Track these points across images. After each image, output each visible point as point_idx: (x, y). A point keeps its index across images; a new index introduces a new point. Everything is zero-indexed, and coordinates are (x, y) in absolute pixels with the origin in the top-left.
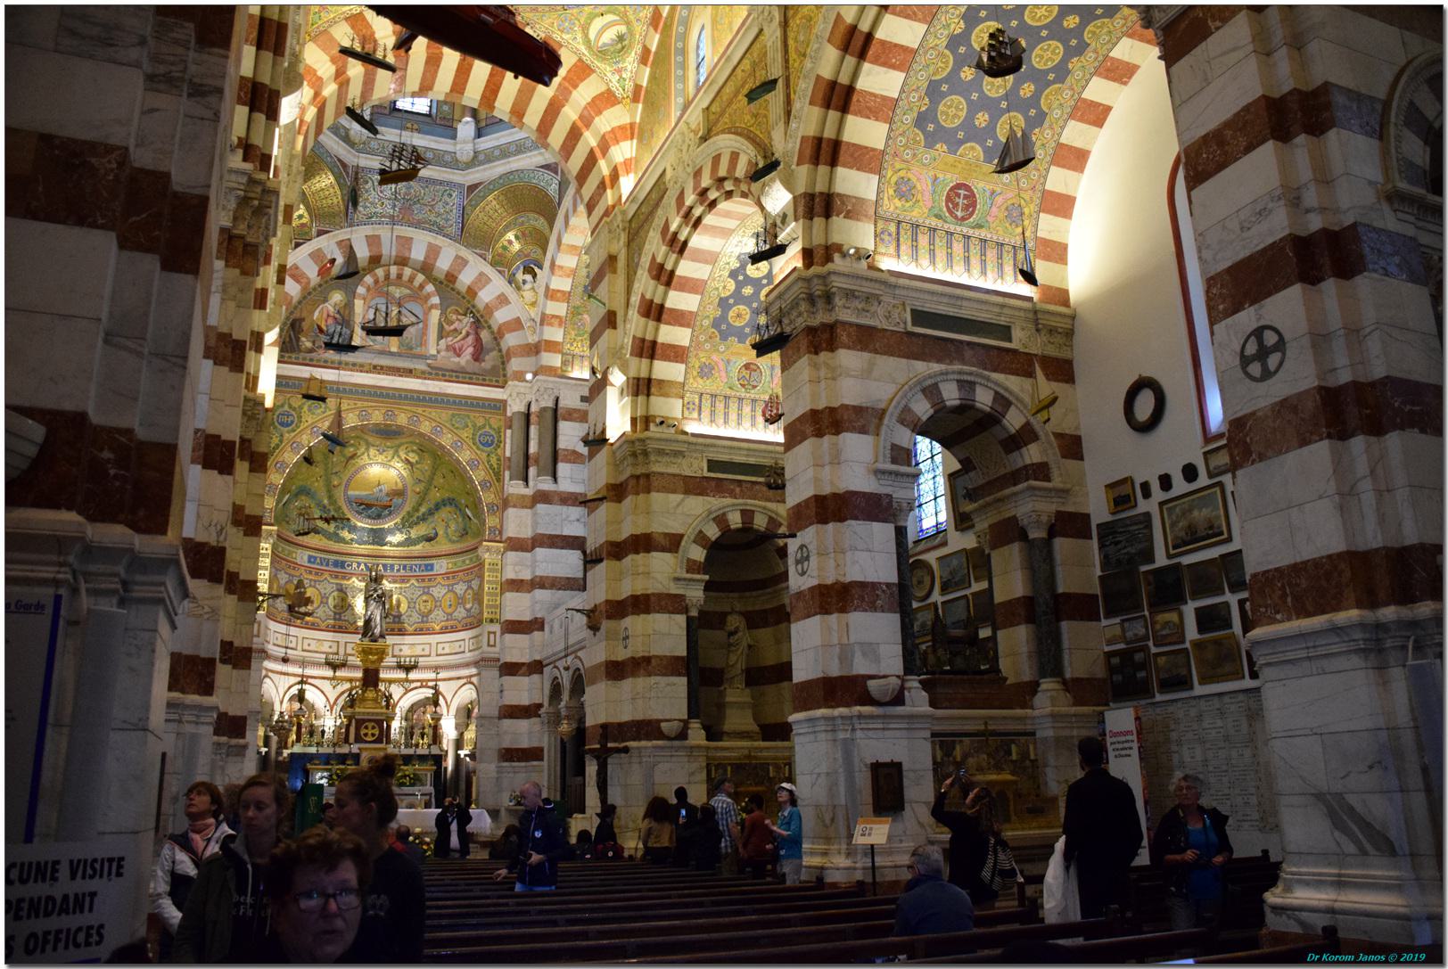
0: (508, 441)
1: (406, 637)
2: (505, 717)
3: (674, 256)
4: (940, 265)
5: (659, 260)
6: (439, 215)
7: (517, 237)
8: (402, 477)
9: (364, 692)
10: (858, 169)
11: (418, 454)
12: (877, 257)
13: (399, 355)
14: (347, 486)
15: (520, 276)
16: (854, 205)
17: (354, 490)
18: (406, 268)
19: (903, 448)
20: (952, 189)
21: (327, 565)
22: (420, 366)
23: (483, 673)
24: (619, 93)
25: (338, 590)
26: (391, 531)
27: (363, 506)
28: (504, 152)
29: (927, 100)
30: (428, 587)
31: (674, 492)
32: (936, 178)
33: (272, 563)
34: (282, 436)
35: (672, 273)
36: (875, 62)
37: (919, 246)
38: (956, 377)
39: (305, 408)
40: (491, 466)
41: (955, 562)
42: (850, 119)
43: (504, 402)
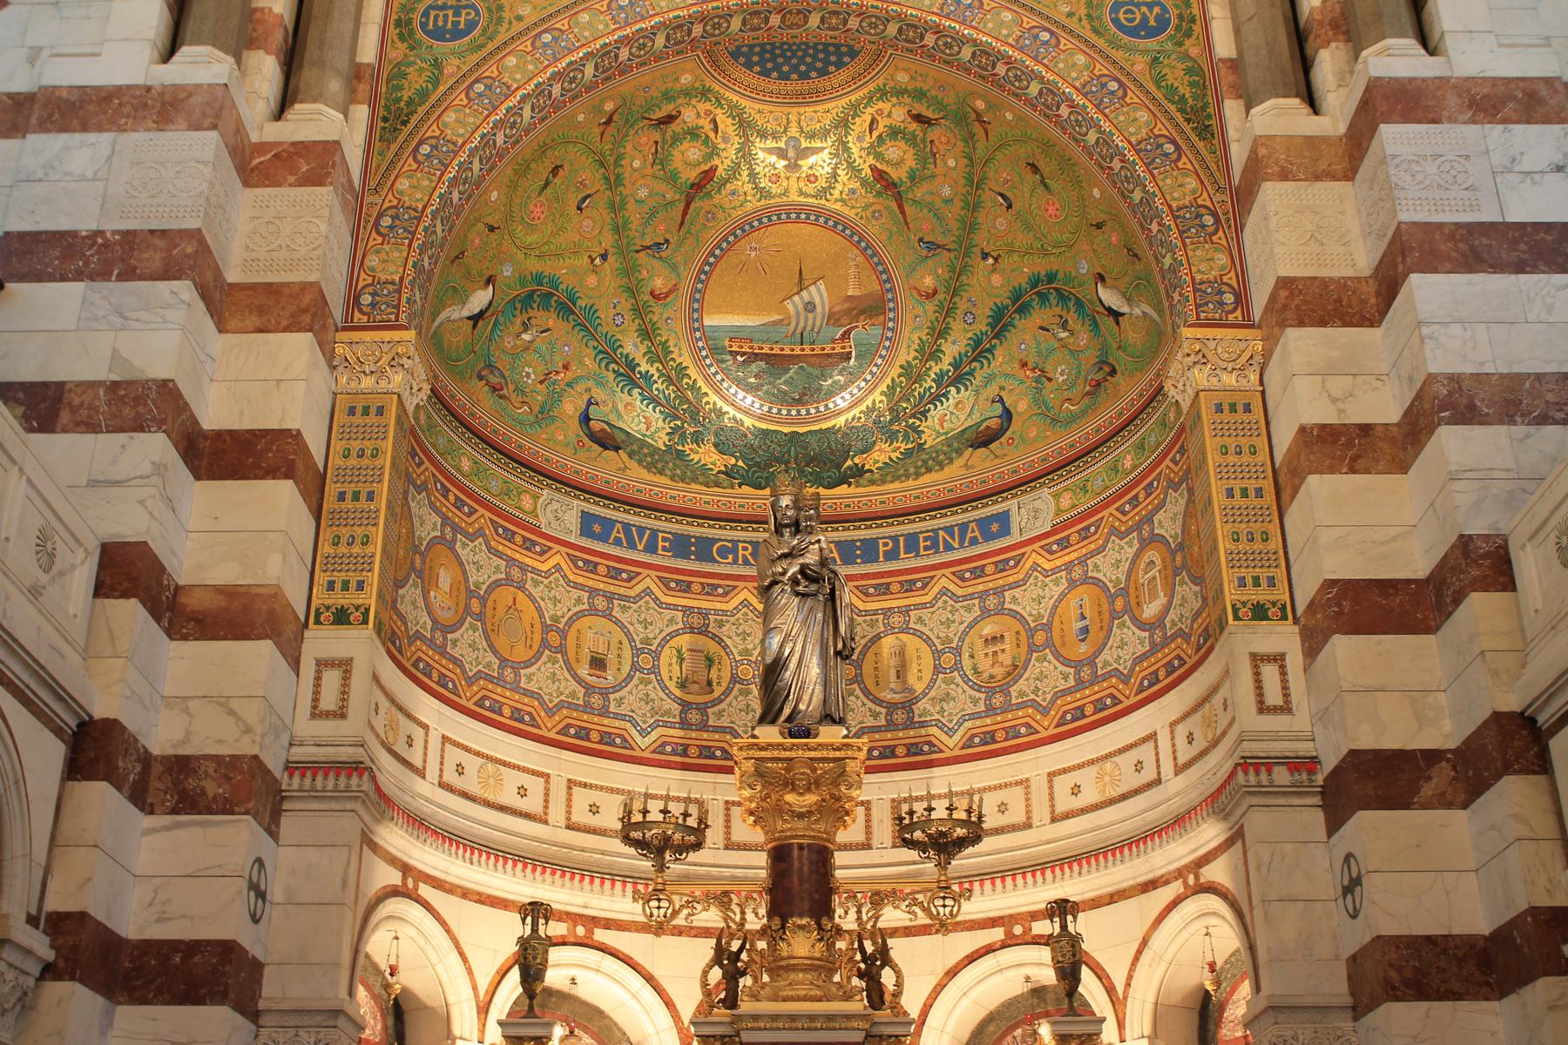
1: (937, 771)
2: (1394, 993)
9: (773, 946)
11: (911, 140)
21: (651, 548)
23: (1258, 822)
25: (691, 630)
27: (754, 367)
30: (999, 592)
34: (437, 64)
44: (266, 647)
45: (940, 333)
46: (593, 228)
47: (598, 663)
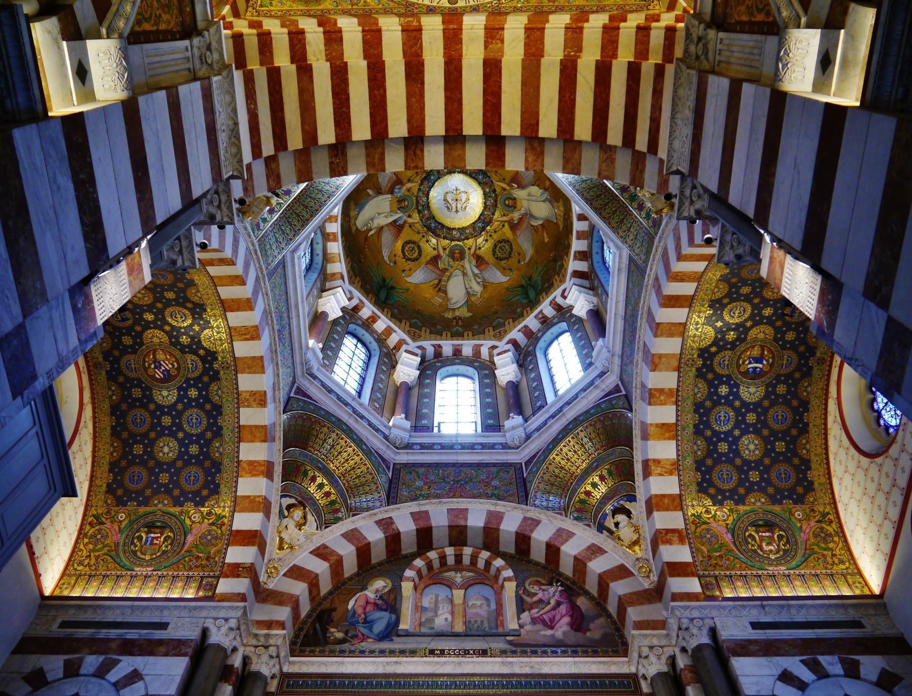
6: (496, 488)
7: (594, 485)
18: (465, 548)
22: (499, 644)
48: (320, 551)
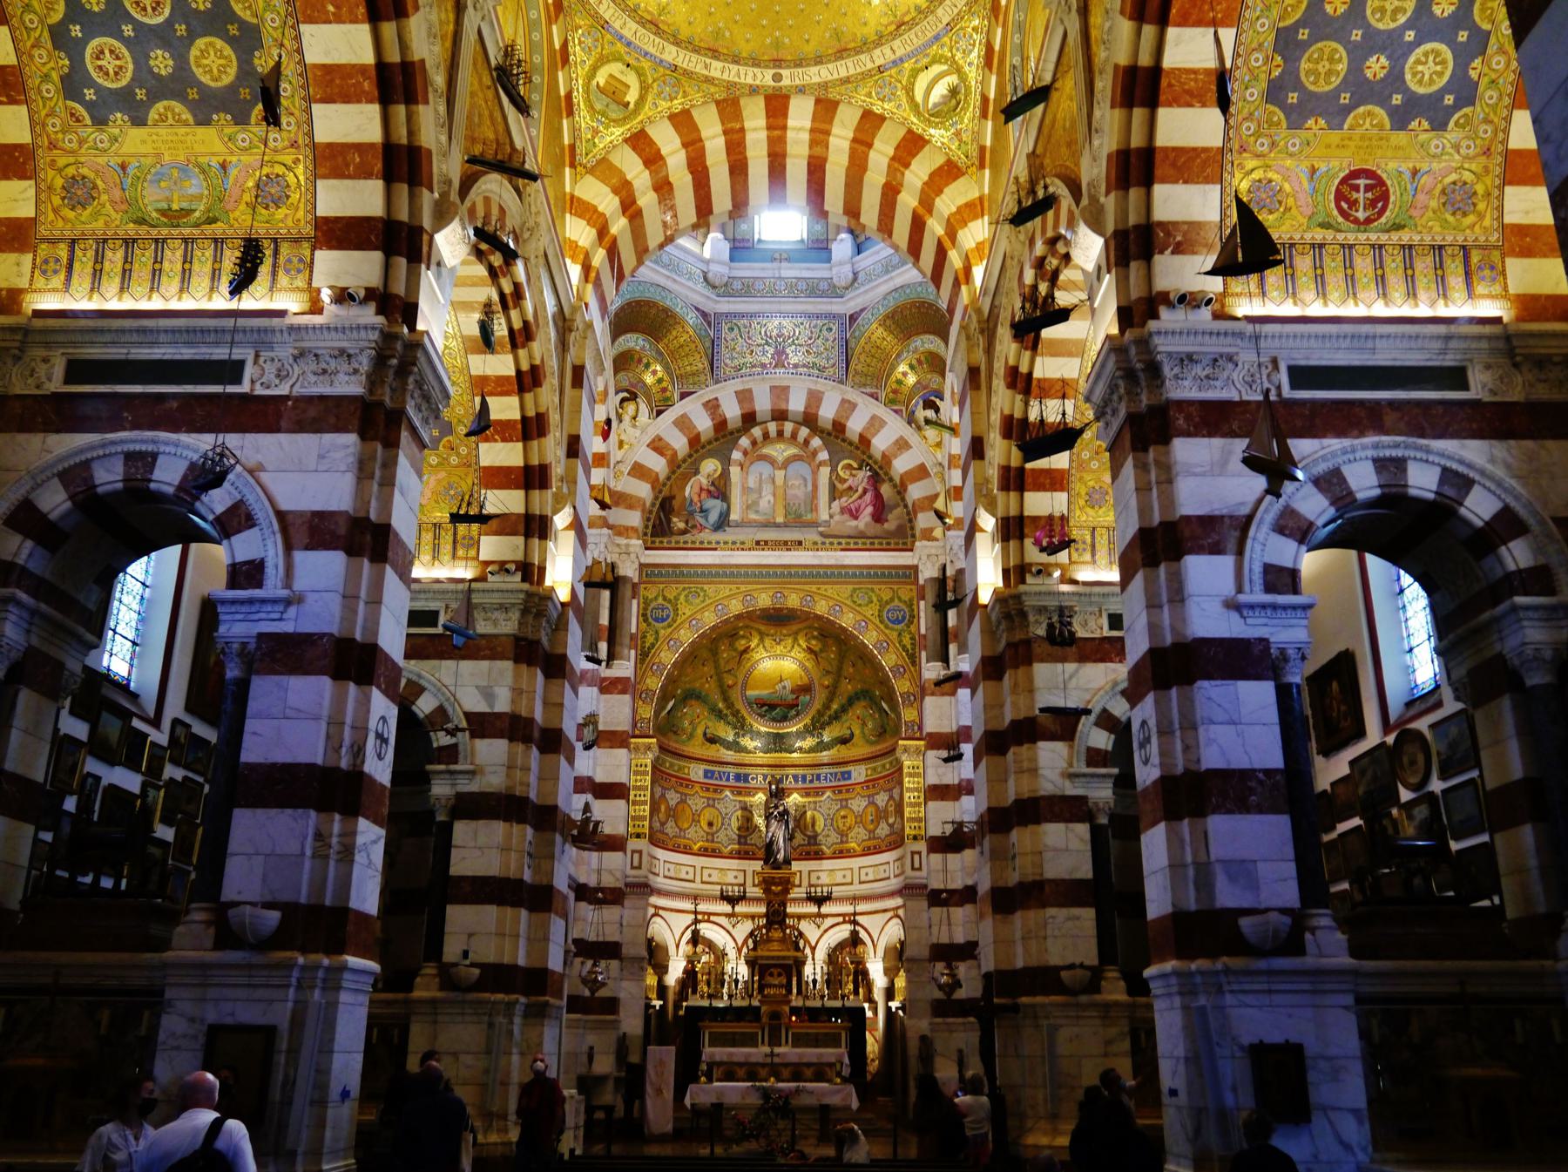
0: (922, 614)
3: (1028, 354)
4: (1334, 295)
5: (1011, 362)
6: (819, 354)
7: (912, 367)
8: (805, 669)
10: (1186, 182)
12: (1228, 301)
13: (785, 525)
14: (745, 686)
15: (922, 414)
16: (1185, 235)
17: (756, 688)
19: (1281, 569)
20: (1344, 181)
22: (810, 536)
23: (909, 904)
24: (961, 160)
26: (800, 735)
28: (888, 268)
29: (1278, 59)
31: (1063, 660)
32: (1313, 170)
33: (653, 782)
35: (1030, 374)
36: (1184, 22)
37: (1298, 274)
38: (1370, 453)
39: (682, 598)
40: (904, 647)
41: (1453, 731)
42: (1163, 113)
43: (915, 568)
44: (620, 854)
45: (830, 700)
46: (708, 669)
47: (710, 824)
48: (657, 444)
